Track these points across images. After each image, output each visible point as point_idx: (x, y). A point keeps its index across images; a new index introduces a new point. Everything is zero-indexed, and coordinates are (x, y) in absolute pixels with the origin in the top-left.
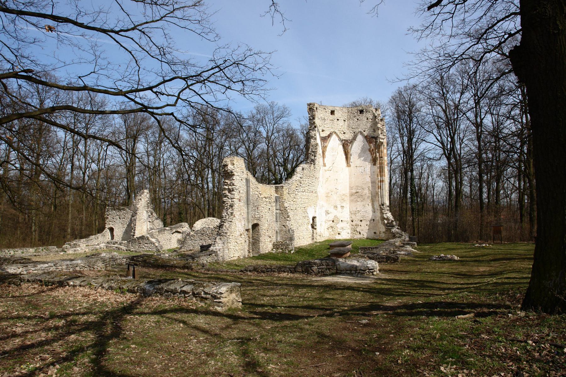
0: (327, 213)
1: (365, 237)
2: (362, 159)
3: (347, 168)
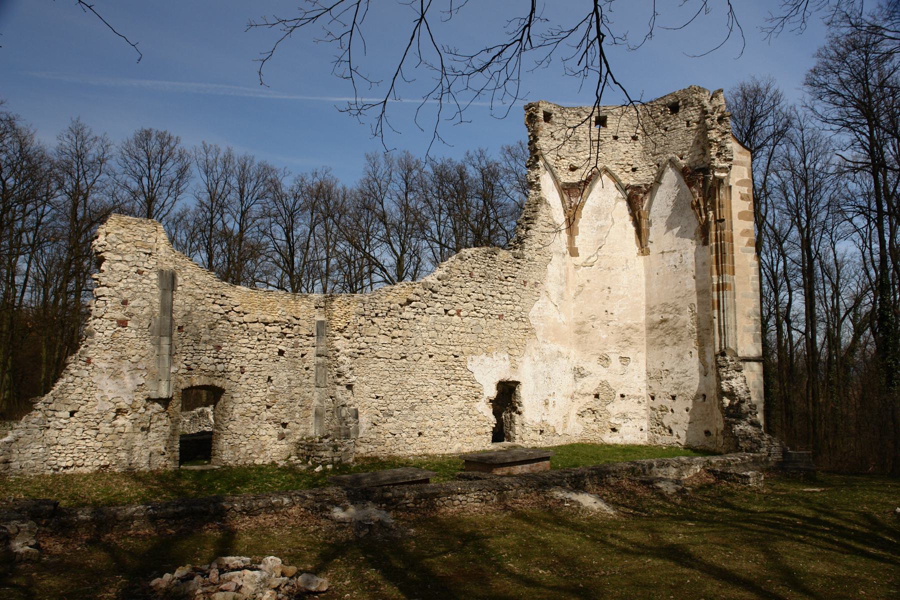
0: (579, 374)
1: (683, 441)
2: (676, 230)
3: (642, 258)
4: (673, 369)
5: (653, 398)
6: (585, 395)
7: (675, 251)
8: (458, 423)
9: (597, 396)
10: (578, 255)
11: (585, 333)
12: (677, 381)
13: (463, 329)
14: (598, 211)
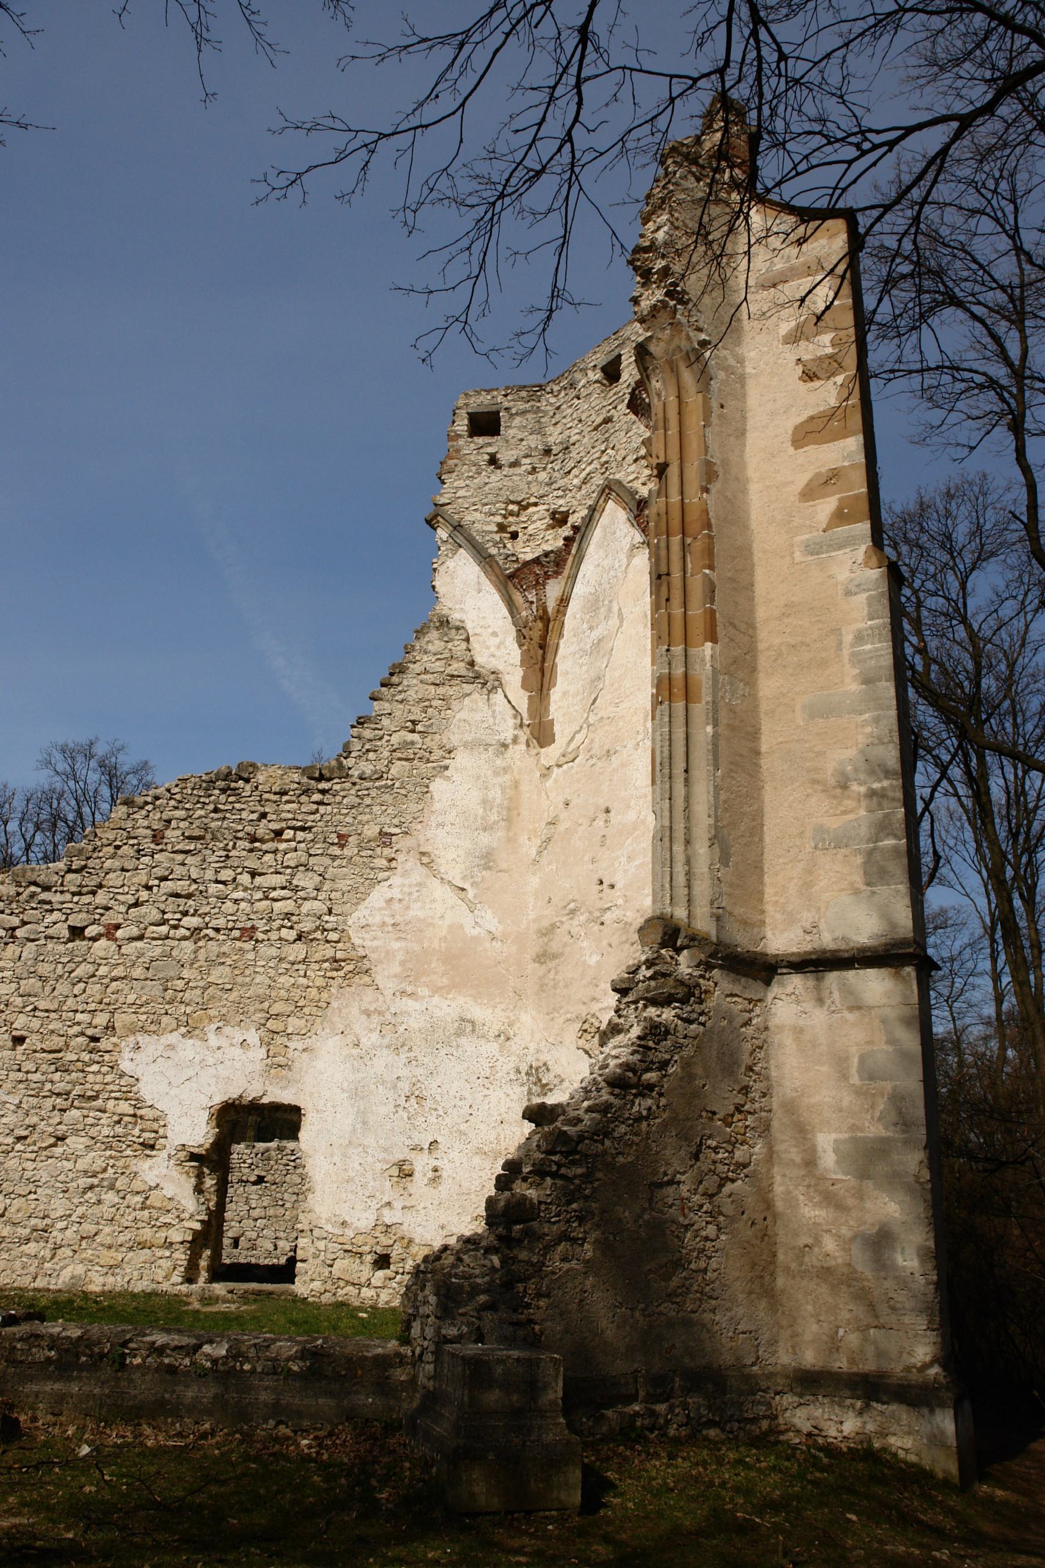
8: (81, 1210)
11: (554, 956)
13: (119, 972)
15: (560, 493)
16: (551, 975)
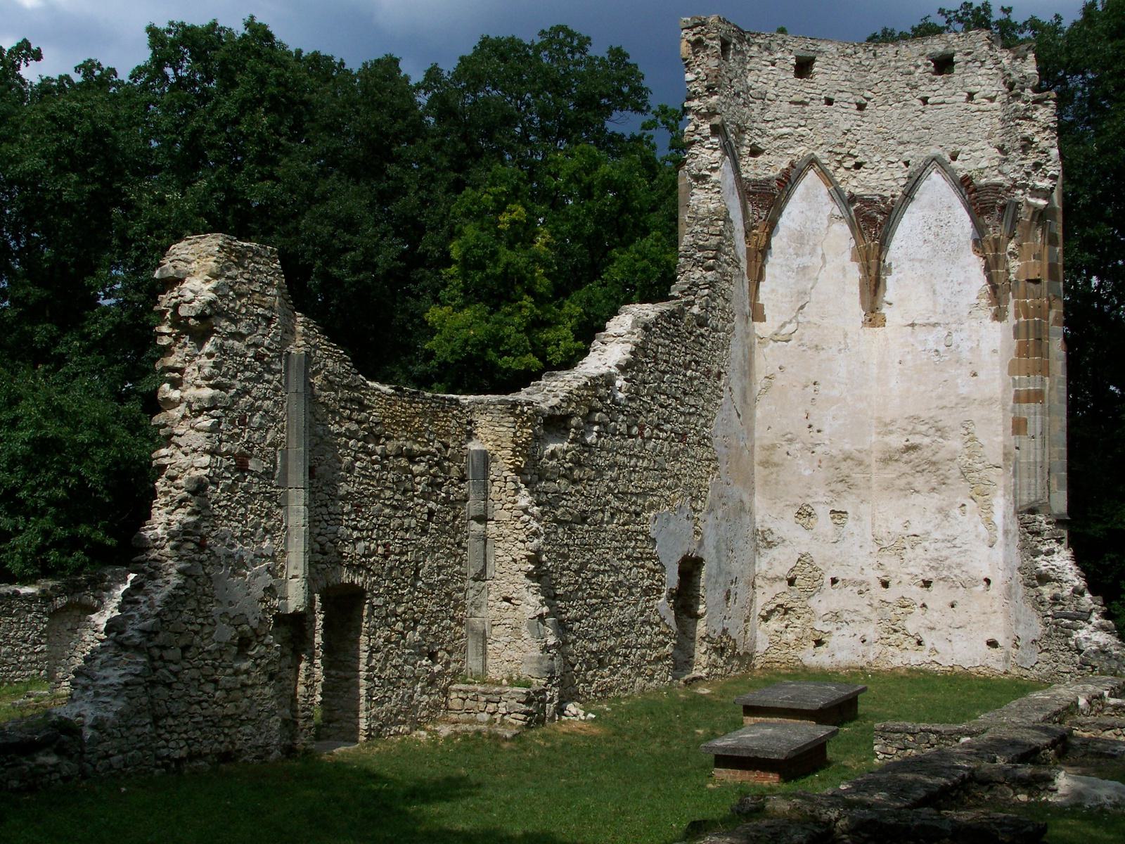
4: (928, 533)
5: (885, 584)
6: (775, 579)
7: (935, 325)
9: (791, 582)
10: (763, 319)
11: (776, 465)
12: (936, 555)
14: (800, 239)
15: (760, 133)
16: (774, 476)
